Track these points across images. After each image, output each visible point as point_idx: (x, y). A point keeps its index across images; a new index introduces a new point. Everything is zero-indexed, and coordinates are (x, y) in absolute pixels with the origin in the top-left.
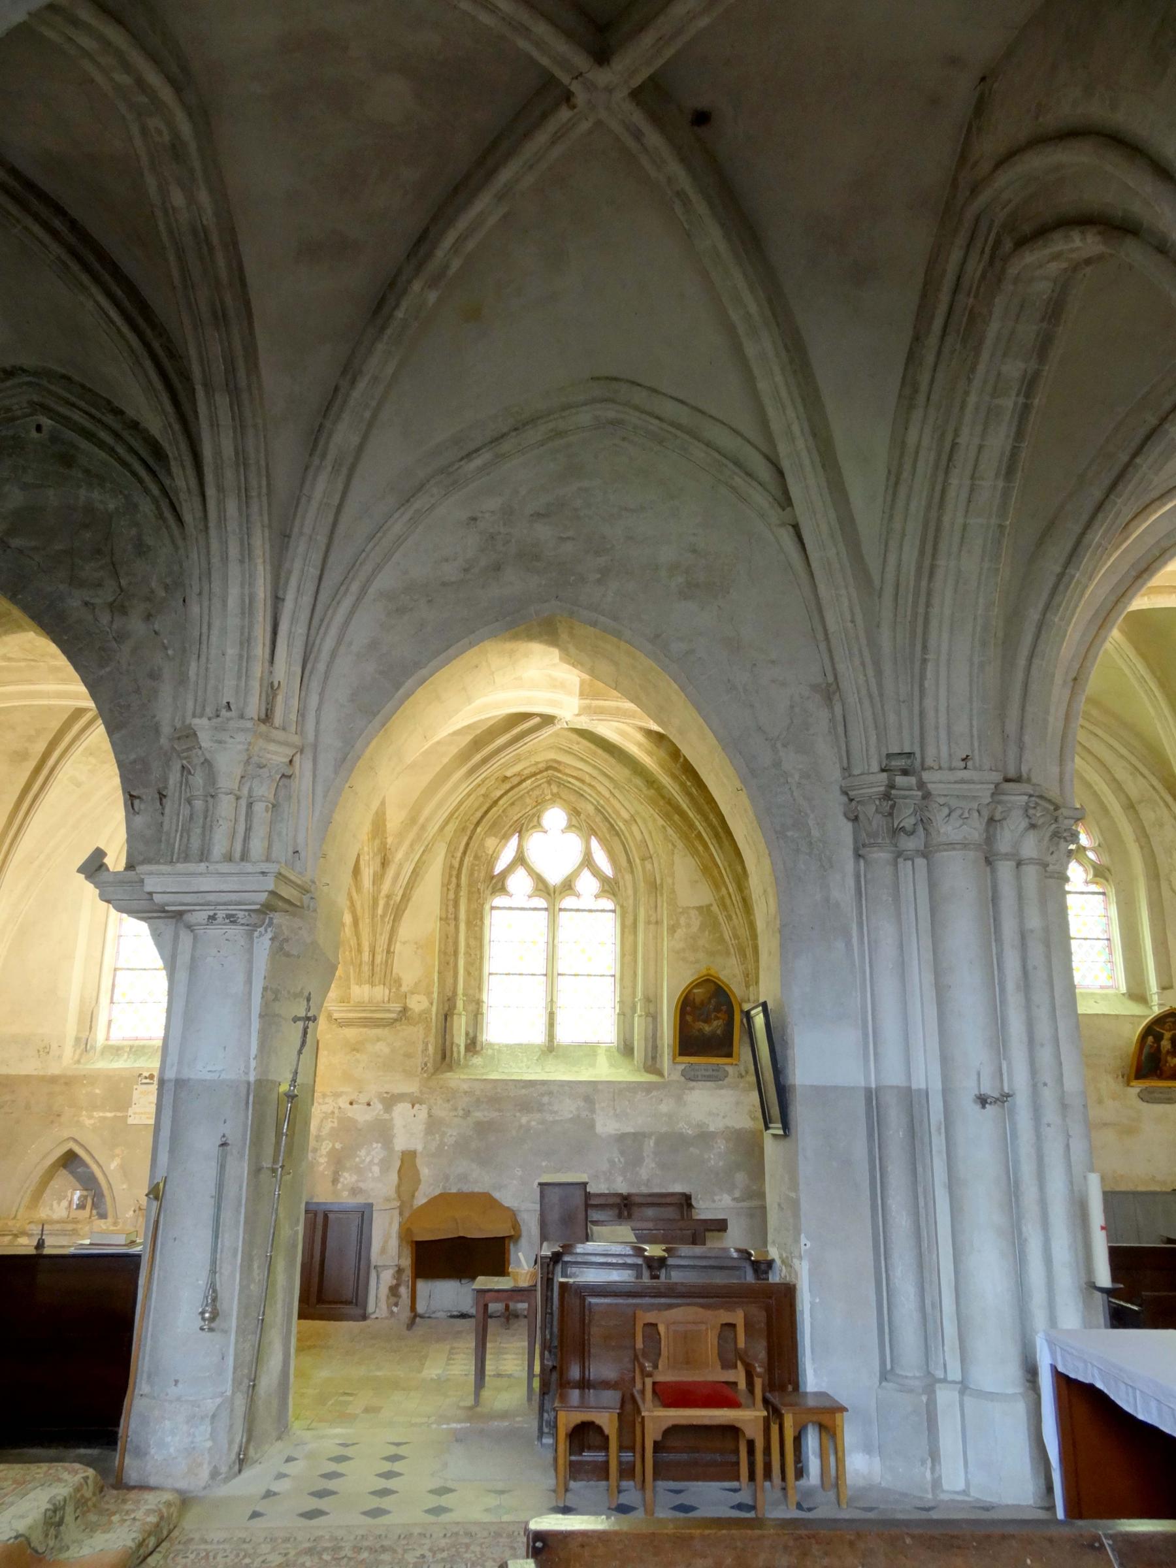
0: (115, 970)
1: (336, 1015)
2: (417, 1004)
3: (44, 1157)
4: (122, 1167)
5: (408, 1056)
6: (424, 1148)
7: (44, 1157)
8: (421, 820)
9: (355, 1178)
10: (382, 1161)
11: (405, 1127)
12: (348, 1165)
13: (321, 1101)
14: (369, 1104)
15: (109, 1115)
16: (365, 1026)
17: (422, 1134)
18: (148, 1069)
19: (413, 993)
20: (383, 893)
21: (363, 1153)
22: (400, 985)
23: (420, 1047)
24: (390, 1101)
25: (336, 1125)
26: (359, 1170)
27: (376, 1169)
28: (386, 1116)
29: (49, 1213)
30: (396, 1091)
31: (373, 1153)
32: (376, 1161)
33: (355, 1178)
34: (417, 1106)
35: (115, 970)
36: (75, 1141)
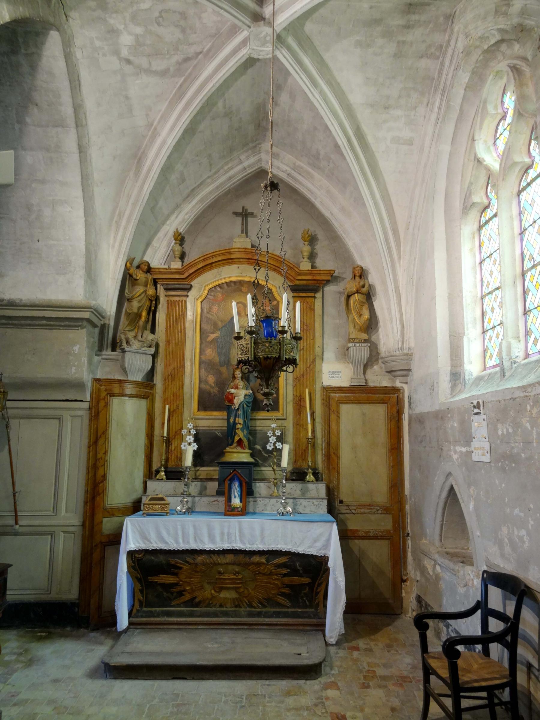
18: (478, 396)
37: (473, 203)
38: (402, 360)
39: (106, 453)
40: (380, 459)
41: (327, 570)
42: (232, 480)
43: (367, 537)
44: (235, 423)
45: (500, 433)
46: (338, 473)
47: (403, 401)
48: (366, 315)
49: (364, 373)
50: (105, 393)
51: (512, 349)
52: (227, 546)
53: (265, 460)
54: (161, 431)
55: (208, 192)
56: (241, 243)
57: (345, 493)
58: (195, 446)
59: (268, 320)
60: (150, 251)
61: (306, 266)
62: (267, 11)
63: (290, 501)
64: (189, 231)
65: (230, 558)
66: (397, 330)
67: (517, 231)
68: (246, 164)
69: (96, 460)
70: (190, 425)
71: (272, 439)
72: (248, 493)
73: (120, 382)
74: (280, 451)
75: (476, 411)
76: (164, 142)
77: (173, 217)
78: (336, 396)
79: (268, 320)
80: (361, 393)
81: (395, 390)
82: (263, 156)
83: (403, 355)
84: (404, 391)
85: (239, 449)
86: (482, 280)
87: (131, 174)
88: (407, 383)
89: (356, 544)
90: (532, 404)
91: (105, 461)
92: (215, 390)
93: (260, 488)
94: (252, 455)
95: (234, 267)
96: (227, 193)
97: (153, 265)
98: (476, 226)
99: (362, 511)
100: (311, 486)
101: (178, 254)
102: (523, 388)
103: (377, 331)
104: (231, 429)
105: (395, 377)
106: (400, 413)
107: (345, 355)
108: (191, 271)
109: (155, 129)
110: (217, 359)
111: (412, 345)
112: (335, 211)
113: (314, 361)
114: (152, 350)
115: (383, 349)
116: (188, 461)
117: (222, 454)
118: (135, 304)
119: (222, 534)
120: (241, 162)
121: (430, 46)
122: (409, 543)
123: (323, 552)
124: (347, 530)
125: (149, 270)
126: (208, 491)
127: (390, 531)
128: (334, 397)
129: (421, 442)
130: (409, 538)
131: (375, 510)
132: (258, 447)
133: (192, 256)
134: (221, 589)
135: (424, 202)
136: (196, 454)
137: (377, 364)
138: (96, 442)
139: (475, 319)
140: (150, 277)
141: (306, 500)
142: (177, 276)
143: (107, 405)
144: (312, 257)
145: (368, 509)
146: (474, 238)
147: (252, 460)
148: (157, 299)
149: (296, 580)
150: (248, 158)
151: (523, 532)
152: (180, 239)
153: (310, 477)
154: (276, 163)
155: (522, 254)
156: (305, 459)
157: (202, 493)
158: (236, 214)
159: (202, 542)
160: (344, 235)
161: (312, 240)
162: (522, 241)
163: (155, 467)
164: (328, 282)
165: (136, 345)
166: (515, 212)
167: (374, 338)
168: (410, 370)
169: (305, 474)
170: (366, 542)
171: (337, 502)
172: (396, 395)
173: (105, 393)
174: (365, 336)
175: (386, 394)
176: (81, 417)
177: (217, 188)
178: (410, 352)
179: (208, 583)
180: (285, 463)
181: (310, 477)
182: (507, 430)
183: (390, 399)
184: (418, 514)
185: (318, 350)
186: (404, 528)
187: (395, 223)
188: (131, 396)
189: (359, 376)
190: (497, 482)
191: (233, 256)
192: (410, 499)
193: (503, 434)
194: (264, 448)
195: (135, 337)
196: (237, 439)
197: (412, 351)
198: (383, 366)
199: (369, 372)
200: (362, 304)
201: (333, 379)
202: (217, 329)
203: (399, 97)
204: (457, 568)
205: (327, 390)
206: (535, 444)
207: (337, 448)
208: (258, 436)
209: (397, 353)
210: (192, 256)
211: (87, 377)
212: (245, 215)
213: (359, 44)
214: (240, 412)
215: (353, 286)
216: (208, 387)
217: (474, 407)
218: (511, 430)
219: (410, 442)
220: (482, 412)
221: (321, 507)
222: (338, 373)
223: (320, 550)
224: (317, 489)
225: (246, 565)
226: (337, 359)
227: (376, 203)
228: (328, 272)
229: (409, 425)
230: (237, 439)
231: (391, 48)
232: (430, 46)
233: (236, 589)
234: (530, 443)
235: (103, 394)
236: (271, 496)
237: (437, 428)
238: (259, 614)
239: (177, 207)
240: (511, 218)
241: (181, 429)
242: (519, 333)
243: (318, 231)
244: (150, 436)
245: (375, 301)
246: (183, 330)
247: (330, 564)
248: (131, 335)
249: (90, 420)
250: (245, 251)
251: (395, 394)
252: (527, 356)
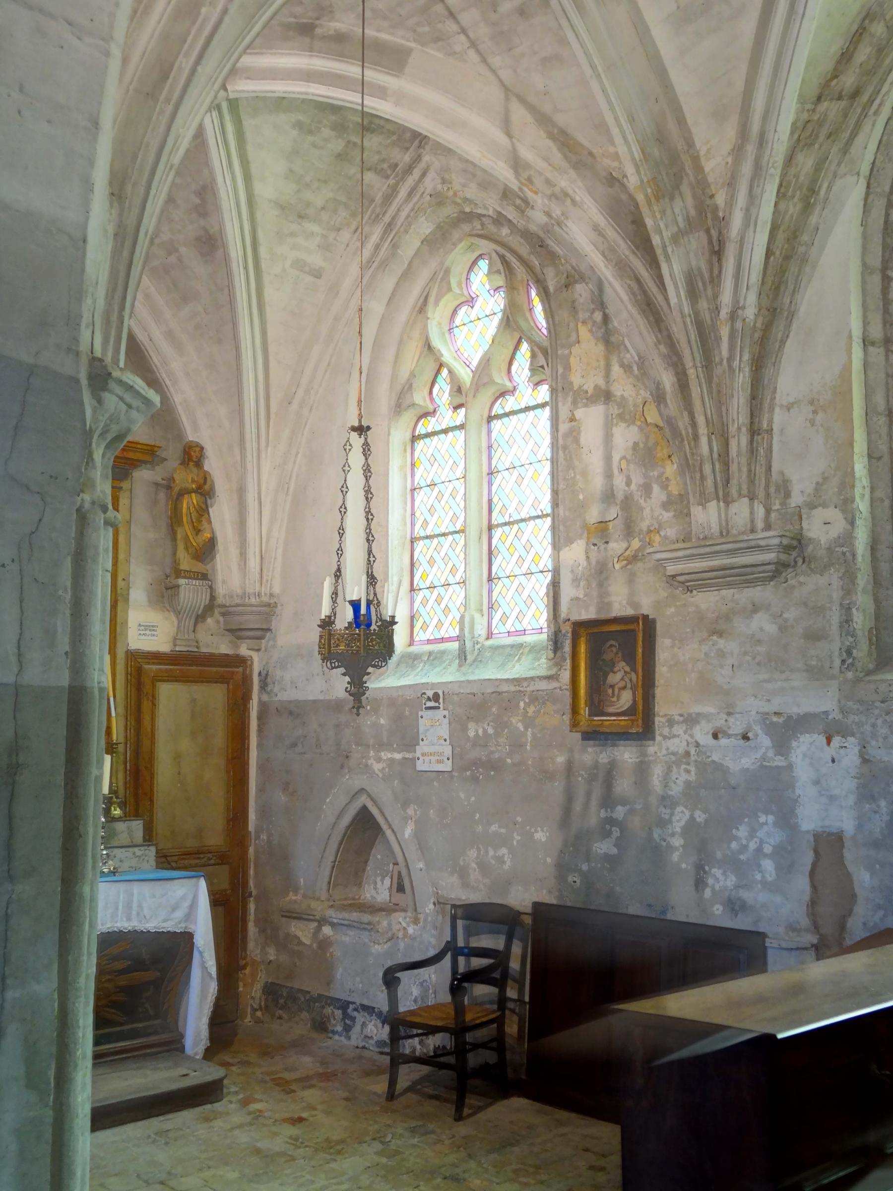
0: (413, 541)
1: (671, 569)
2: (822, 527)
3: (339, 817)
4: (419, 836)
5: (814, 636)
6: (860, 827)
7: (339, 817)
8: (755, 128)
9: (731, 881)
10: (779, 850)
11: (817, 782)
12: (719, 855)
13: (666, 731)
14: (745, 738)
15: (398, 756)
16: (729, 585)
17: (851, 799)
18: (434, 685)
19: (812, 506)
20: (724, 313)
21: (742, 832)
22: (788, 495)
23: (835, 617)
24: (785, 730)
25: (692, 777)
26: (734, 864)
27: (768, 865)
28: (779, 761)
29: (373, 892)
30: (795, 710)
31: (761, 834)
32: (768, 849)
33: (731, 881)
34: (836, 741)
35: (413, 541)
36: (369, 796)
37: (414, 404)
38: (259, 613)
40: (214, 775)
45: (471, 733)
47: (252, 680)
51: (476, 626)
67: (485, 470)
75: (432, 704)
80: (186, 665)
83: (262, 606)
84: (252, 663)
86: (413, 514)
88: (258, 650)
90: (527, 701)
98: (408, 435)
99: (186, 862)
102: (517, 681)
103: (213, 558)
105: (239, 638)
106: (246, 698)
107: (163, 597)
111: (277, 590)
112: (157, 334)
115: (221, 591)
121: (384, 160)
122: (252, 907)
123: (183, 925)
127: (225, 890)
129: (294, 745)
130: (252, 899)
131: (205, 859)
135: (326, 371)
137: (212, 616)
139: (402, 569)
141: (123, 850)
145: (195, 858)
146: (405, 450)
151: (504, 851)
155: (490, 501)
160: (168, 382)
162: (490, 484)
166: (484, 445)
168: (269, 630)
172: (241, 669)
175: (226, 667)
178: (272, 601)
182: (485, 731)
183: (229, 676)
184: (280, 858)
186: (245, 884)
189: (187, 636)
190: (462, 796)
192: (257, 837)
193: (477, 735)
197: (275, 600)
198: (221, 619)
199: (200, 626)
201: (146, 637)
203: (323, 208)
204: (377, 919)
205: (136, 659)
206: (528, 748)
207: (151, 758)
209: (253, 601)
213: (299, 125)
217: (429, 699)
218: (490, 731)
219: (260, 746)
220: (441, 706)
221: (146, 858)
222: (151, 628)
223: (180, 922)
224: (130, 832)
226: (150, 601)
228: (149, 448)
229: (259, 718)
231: (338, 145)
232: (384, 160)
234: (521, 746)
237: (337, 726)
240: (480, 451)
242: (481, 605)
245: (212, 506)
251: (238, 667)
252: (490, 635)
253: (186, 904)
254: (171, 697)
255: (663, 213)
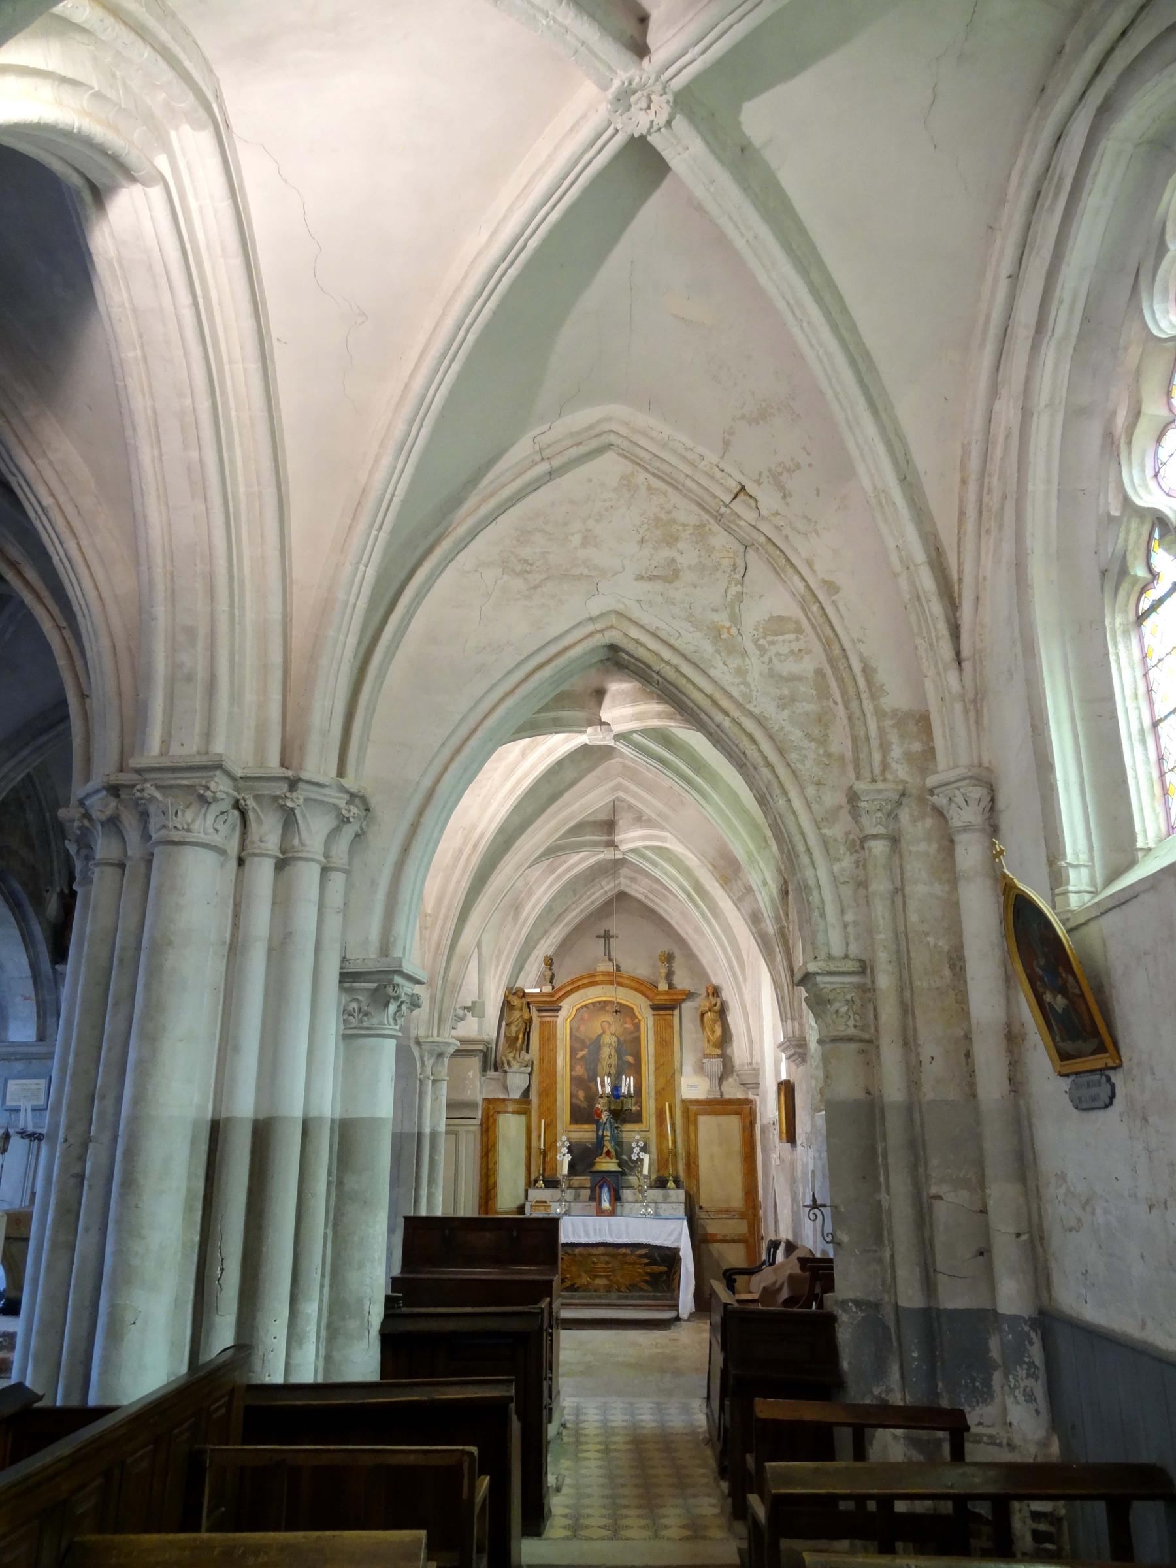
39: (495, 1163)
40: (735, 1169)
41: (680, 1260)
42: (601, 1187)
43: (724, 1241)
44: (603, 1136)
46: (698, 1181)
48: (719, 1032)
49: (720, 1085)
50: (491, 1111)
52: (599, 1240)
53: (632, 1169)
54: (539, 1143)
55: (573, 916)
56: (604, 966)
57: (704, 1199)
58: (568, 1158)
59: (616, 1088)
60: (522, 974)
61: (663, 986)
62: (617, 838)
63: (653, 1205)
64: (555, 953)
65: (601, 1250)
66: (745, 1045)
68: (606, 888)
69: (488, 1169)
70: (564, 1138)
71: (637, 1150)
72: (616, 1198)
73: (504, 1100)
74: (641, 1160)
76: (539, 900)
77: (542, 942)
78: (694, 1108)
79: (616, 1088)
80: (718, 1105)
81: (748, 1101)
82: (622, 880)
85: (608, 1159)
87: (510, 918)
89: (715, 1248)
91: (495, 1170)
92: (584, 1105)
93: (627, 1194)
94: (620, 1165)
95: (599, 987)
96: (591, 915)
97: (527, 991)
100: (672, 1192)
101: (548, 978)
104: (600, 1141)
106: (752, 1123)
108: (561, 993)
109: (531, 888)
110: (586, 1076)
112: (690, 931)
113: (673, 1076)
114: (528, 1070)
116: (565, 1170)
117: (593, 1164)
118: (514, 1029)
119: (595, 1230)
120: (602, 888)
124: (706, 1235)
125: (524, 995)
126: (581, 1198)
128: (693, 1110)
132: (625, 1157)
133: (561, 980)
134: (596, 1276)
136: (572, 1165)
138: (487, 1154)
140: (525, 1001)
142: (548, 999)
143: (495, 1121)
144: (669, 975)
147: (617, 1169)
148: (531, 1019)
149: (656, 1269)
150: (608, 883)
152: (549, 962)
153: (671, 1184)
154: (634, 886)
156: (667, 1168)
157: (577, 1198)
158: (599, 937)
159: (579, 1236)
161: (669, 958)
163: (533, 1178)
164: (684, 1000)
165: (515, 1066)
167: (728, 1052)
169: (667, 1181)
170: (726, 1245)
171: (697, 1208)
173: (491, 1111)
174: (719, 1052)
176: (473, 1132)
177: (581, 911)
179: (585, 1272)
180: (646, 1171)
181: (671, 1184)
185: (677, 1065)
187: (739, 949)
188: (513, 1112)
191: (598, 979)
194: (630, 1158)
195: (514, 1058)
196: (605, 1150)
199: (724, 1083)
200: (715, 1022)
202: (586, 1051)
205: (685, 1102)
207: (697, 1156)
208: (625, 1148)
210: (561, 980)
211: (479, 1099)
212: (607, 936)
214: (607, 1126)
215: (706, 1004)
216: (578, 1102)
222: (694, 1086)
224: (677, 1196)
225: (614, 1256)
226: (695, 1072)
227: (718, 938)
230: (605, 1150)
233: (607, 1277)
235: (492, 1112)
236: (636, 1202)
238: (626, 1298)
239: (546, 932)
241: (556, 1142)
243: (674, 951)
244: (529, 1148)
246: (554, 1050)
247: (682, 1254)
248: (512, 1055)
249: (482, 1135)
250: (608, 974)
253: (676, 1233)
254: (707, 1125)
255: (731, 889)
